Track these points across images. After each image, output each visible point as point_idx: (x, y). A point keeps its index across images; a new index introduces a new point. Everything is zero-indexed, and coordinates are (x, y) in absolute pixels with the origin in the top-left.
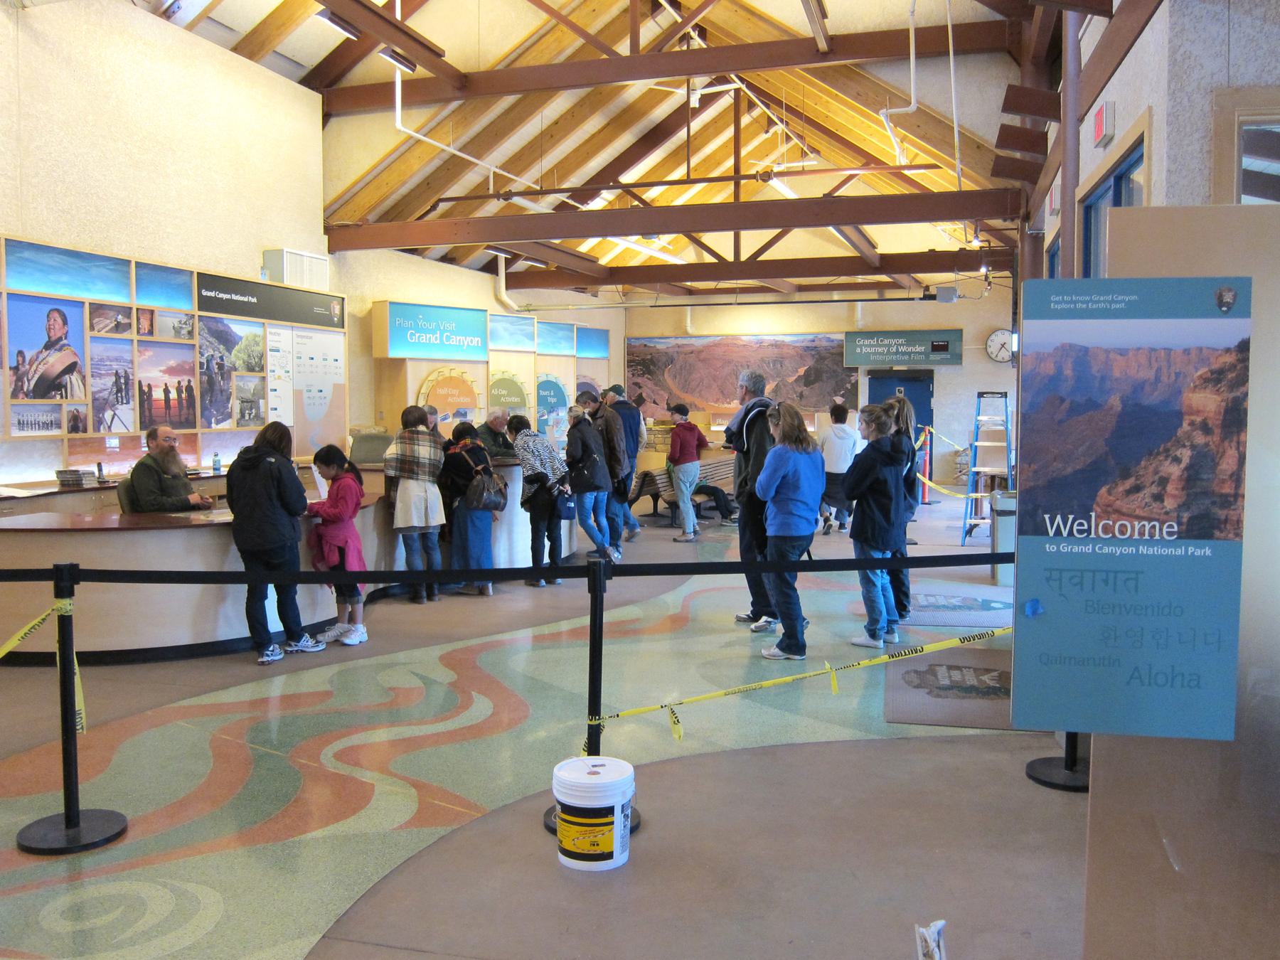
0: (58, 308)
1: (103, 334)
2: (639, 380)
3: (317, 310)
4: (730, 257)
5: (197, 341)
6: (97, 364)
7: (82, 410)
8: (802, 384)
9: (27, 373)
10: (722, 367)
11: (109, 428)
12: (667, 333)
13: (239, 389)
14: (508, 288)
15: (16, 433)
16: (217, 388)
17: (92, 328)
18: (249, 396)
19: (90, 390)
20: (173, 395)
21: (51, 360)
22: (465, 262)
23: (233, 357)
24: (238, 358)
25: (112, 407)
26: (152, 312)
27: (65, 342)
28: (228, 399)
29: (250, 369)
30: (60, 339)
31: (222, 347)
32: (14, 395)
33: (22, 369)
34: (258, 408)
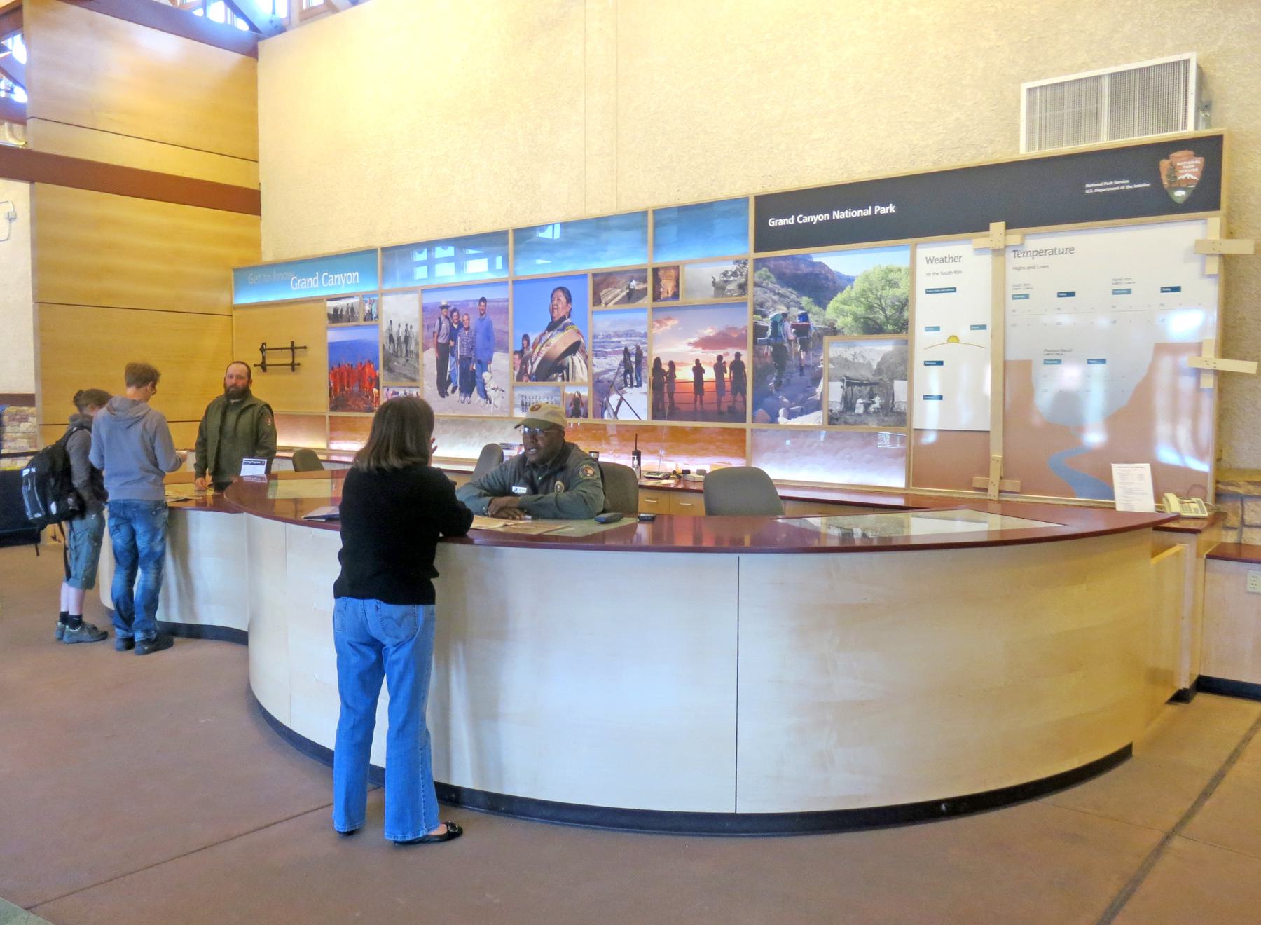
0: (563, 289)
9: (530, 356)
11: (615, 413)
16: (792, 363)
17: (597, 300)
20: (709, 375)
21: (553, 341)
25: (619, 390)
26: (677, 268)
27: (568, 320)
28: (816, 380)
29: (872, 328)
30: (563, 318)
31: (805, 300)
32: (519, 378)
33: (527, 353)
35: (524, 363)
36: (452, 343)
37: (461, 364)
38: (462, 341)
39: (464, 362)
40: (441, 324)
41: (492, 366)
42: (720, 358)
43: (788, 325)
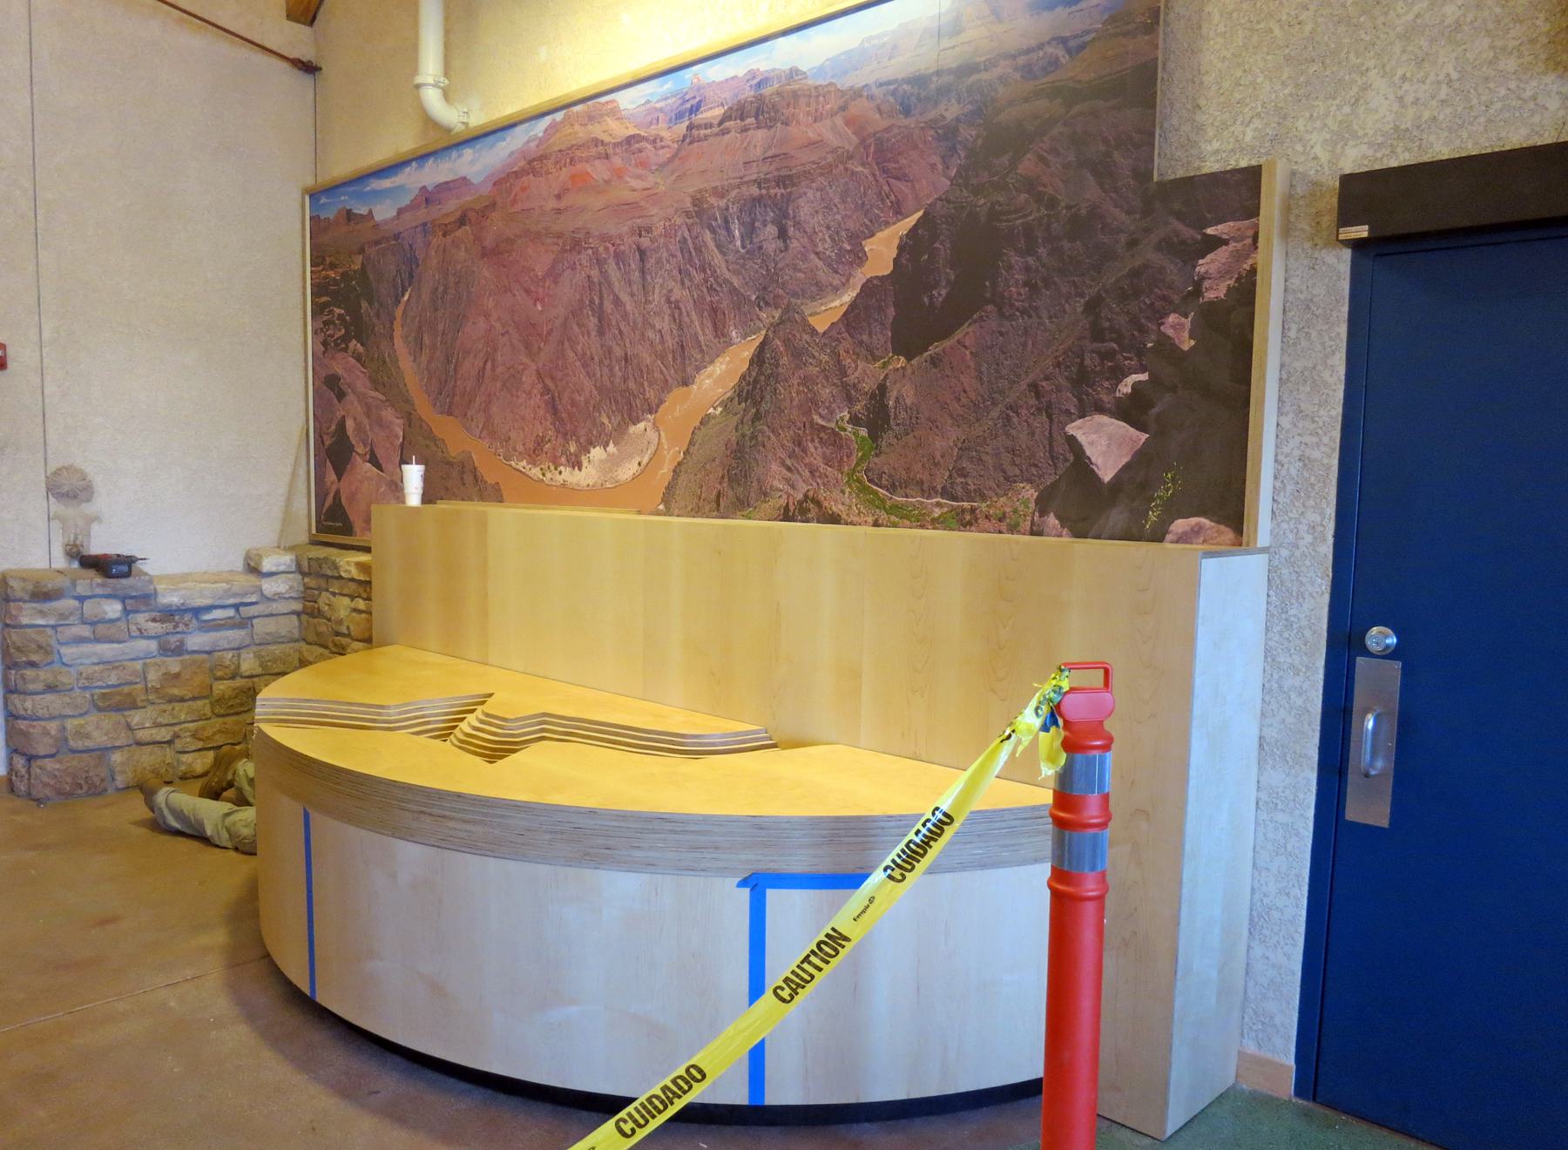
2: (341, 365)
8: (881, 337)
10: (553, 274)
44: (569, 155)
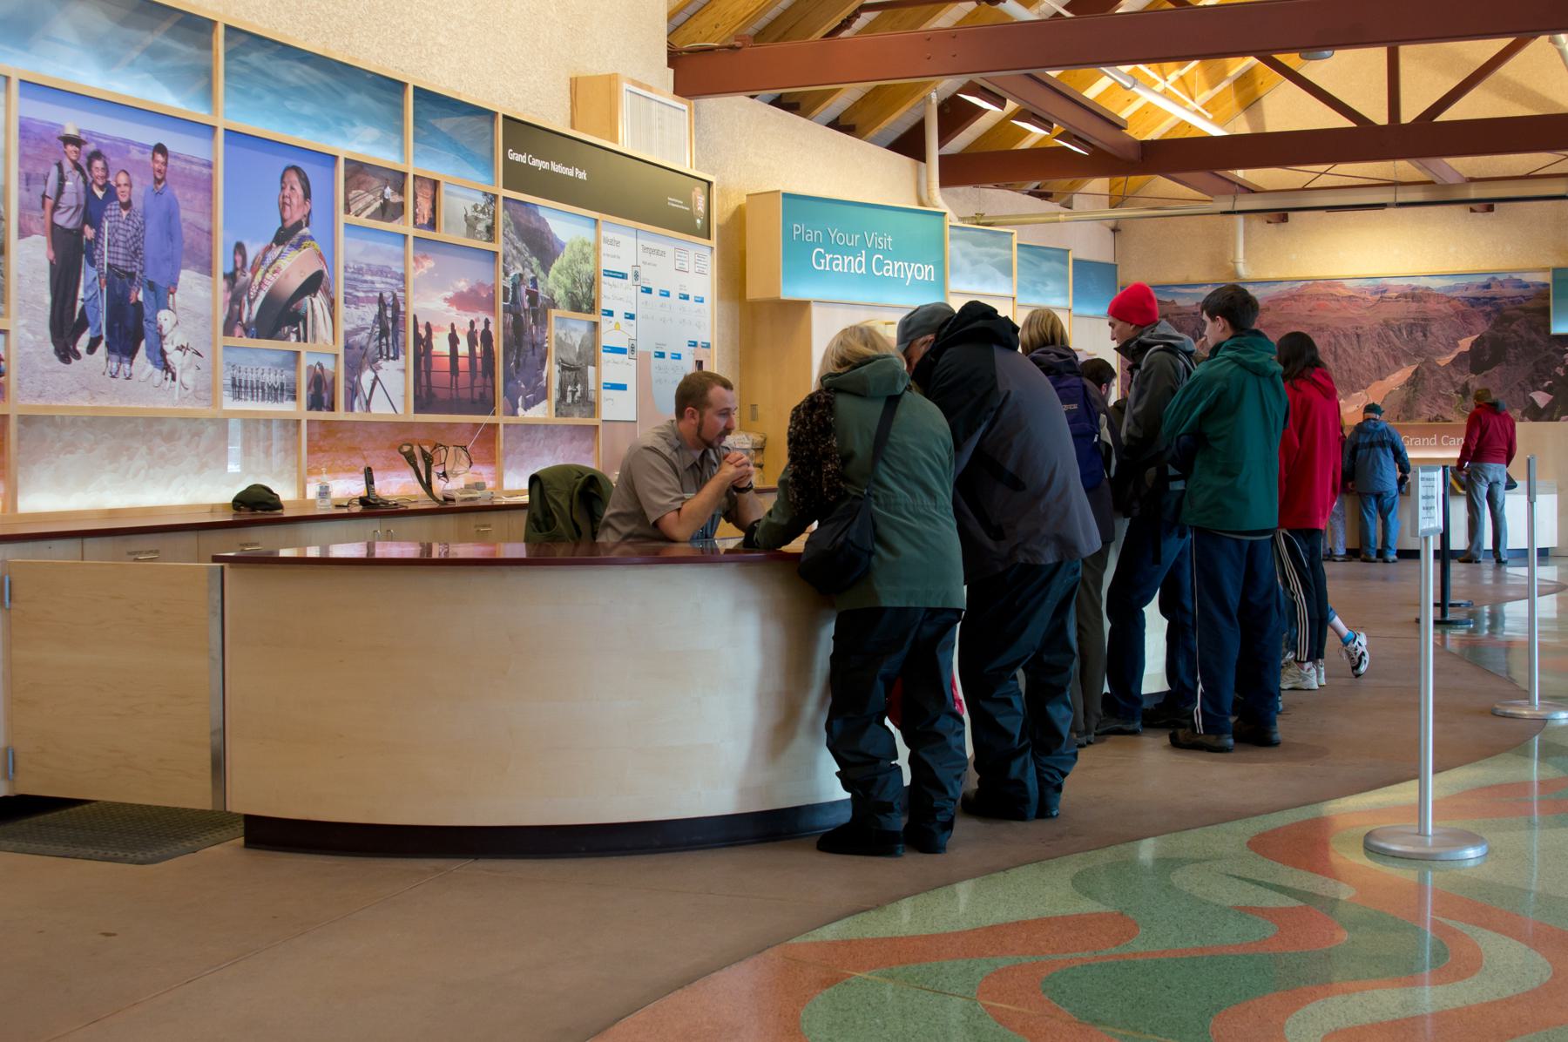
0: (300, 167)
1: (363, 220)
3: (675, 203)
4: (1380, 117)
5: (499, 246)
6: (356, 276)
7: (328, 365)
9: (247, 287)
11: (368, 403)
12: (1196, 277)
13: (561, 344)
14: (945, 181)
15: (229, 404)
16: (526, 338)
18: (571, 358)
19: (343, 327)
20: (463, 348)
21: (284, 264)
22: (873, 133)
23: (551, 283)
24: (557, 281)
27: (305, 231)
28: (543, 361)
29: (576, 307)
31: (535, 261)
32: (228, 330)
33: (242, 280)
34: (585, 383)
35: (236, 299)
36: (89, 233)
37: (110, 284)
38: (114, 230)
39: (118, 281)
40: (62, 179)
41: (178, 298)
42: (472, 324)
43: (524, 289)
44: (1317, 297)
